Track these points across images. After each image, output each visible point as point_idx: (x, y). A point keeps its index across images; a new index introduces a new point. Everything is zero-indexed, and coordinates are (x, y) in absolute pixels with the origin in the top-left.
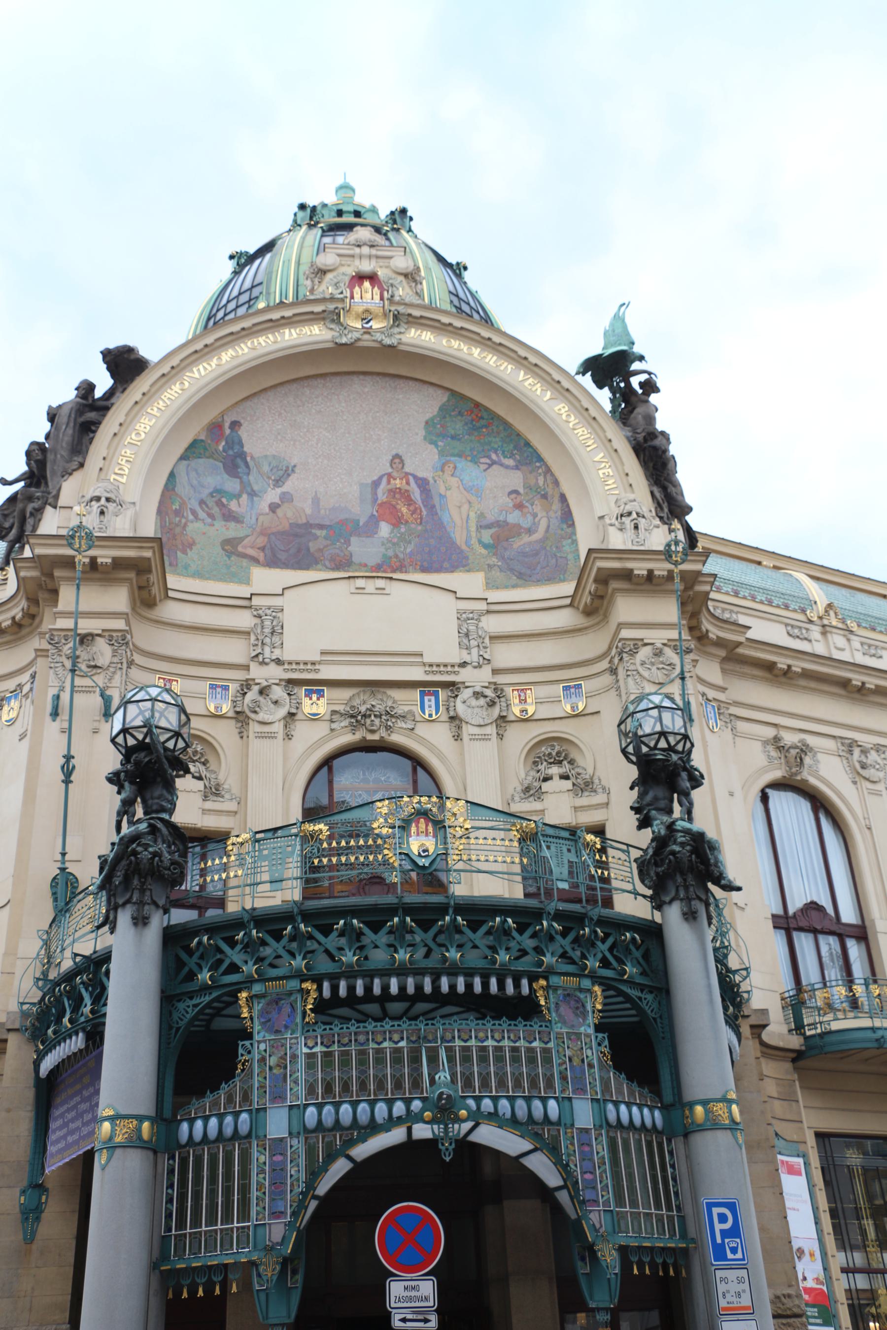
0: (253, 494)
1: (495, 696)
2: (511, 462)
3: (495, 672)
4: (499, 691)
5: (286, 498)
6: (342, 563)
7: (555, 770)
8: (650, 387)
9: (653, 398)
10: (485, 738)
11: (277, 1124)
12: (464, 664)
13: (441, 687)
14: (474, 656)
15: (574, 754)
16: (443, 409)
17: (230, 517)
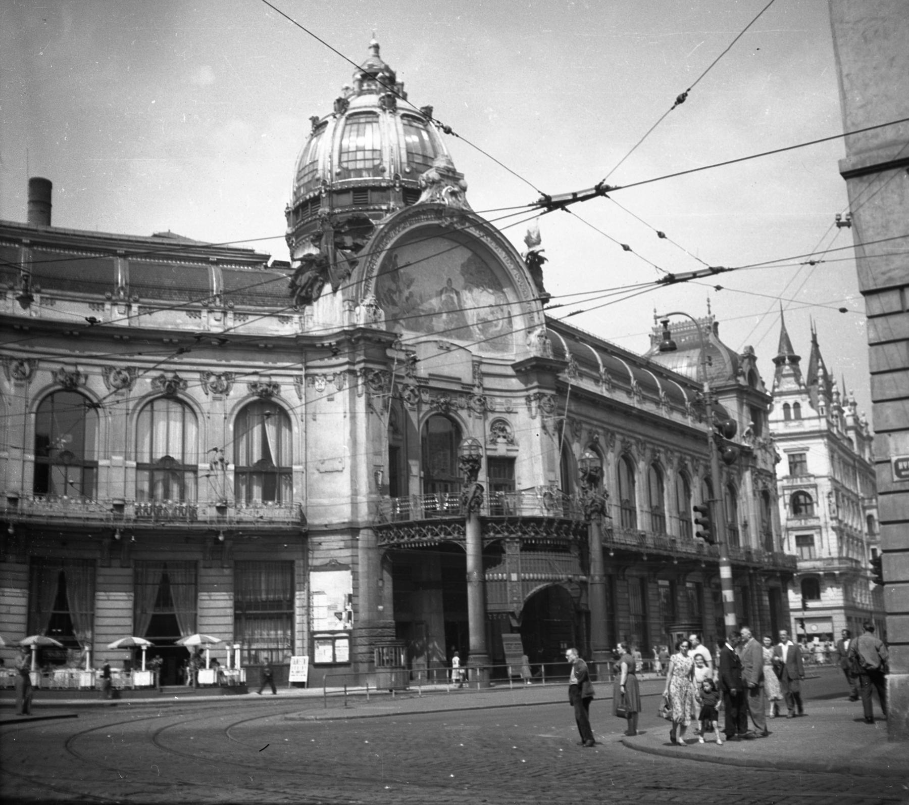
0: (400, 292)
1: (482, 401)
2: (491, 291)
3: (485, 389)
4: (485, 399)
5: (411, 294)
6: (431, 332)
7: (501, 434)
8: (542, 260)
9: (542, 266)
10: (480, 418)
11: (514, 577)
12: (474, 386)
13: (466, 392)
14: (477, 382)
15: (507, 428)
16: (469, 260)
17: (394, 303)
